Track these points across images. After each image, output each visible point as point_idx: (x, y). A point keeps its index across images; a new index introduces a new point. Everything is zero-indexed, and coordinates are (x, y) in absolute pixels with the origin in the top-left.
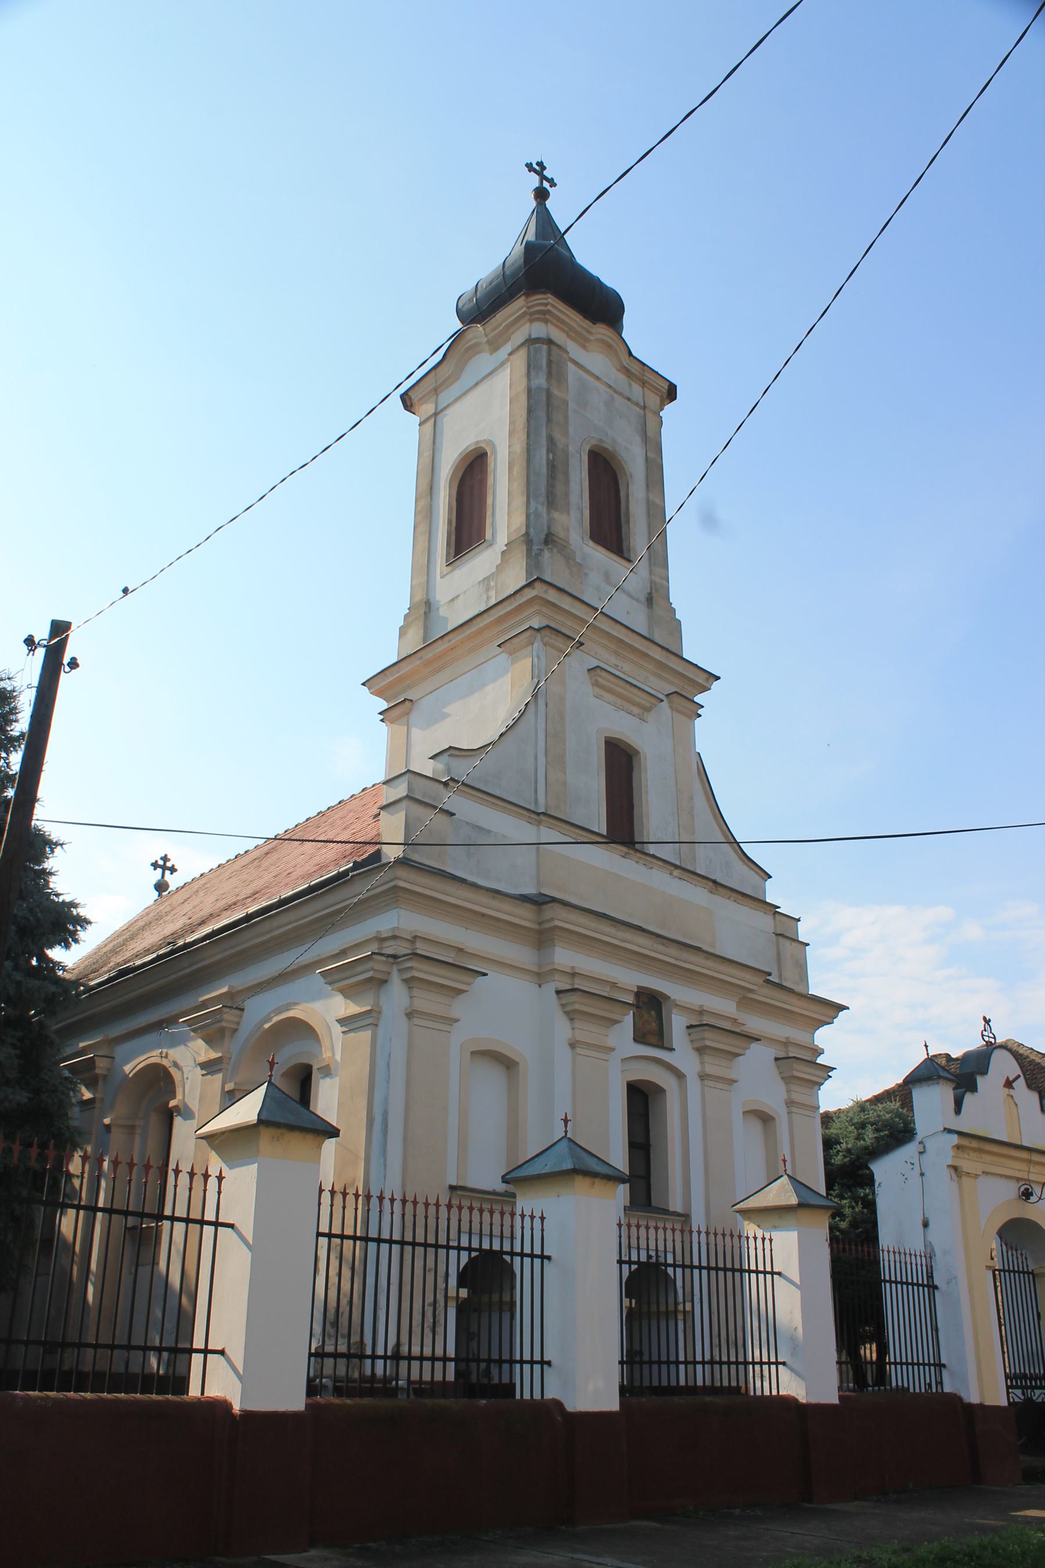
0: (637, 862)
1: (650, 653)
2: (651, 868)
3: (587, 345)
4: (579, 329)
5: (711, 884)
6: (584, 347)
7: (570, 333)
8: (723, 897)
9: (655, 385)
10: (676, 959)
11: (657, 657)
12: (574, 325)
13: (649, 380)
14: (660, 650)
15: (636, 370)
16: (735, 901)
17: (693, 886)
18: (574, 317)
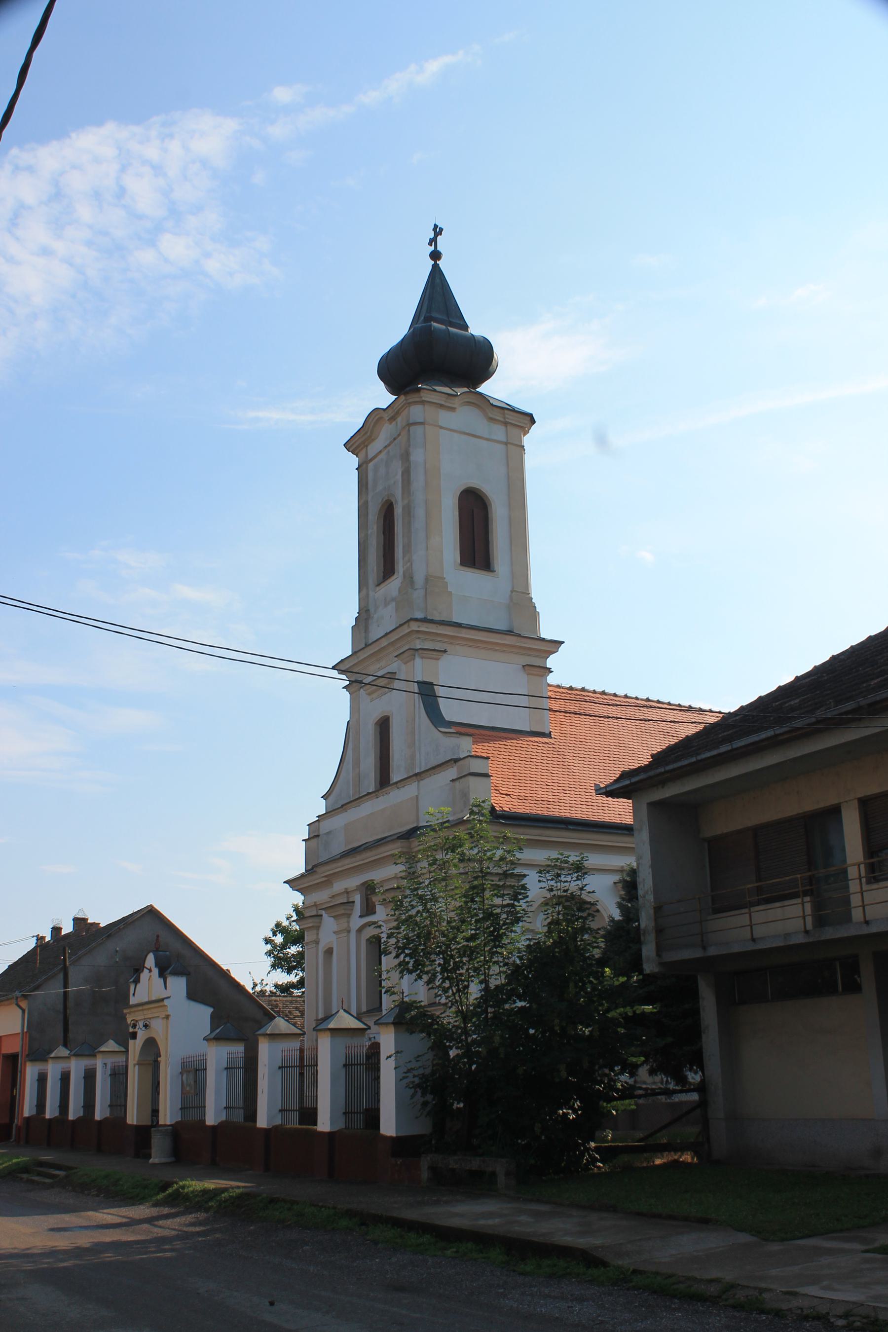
0: (383, 795)
1: (382, 646)
2: (389, 793)
3: (373, 438)
4: (364, 438)
5: (414, 777)
6: (373, 440)
7: (366, 444)
8: (428, 777)
9: (402, 404)
10: (363, 860)
11: (385, 644)
12: (360, 441)
13: (397, 409)
14: (383, 639)
15: (392, 413)
16: (435, 774)
17: (410, 785)
18: (356, 439)
